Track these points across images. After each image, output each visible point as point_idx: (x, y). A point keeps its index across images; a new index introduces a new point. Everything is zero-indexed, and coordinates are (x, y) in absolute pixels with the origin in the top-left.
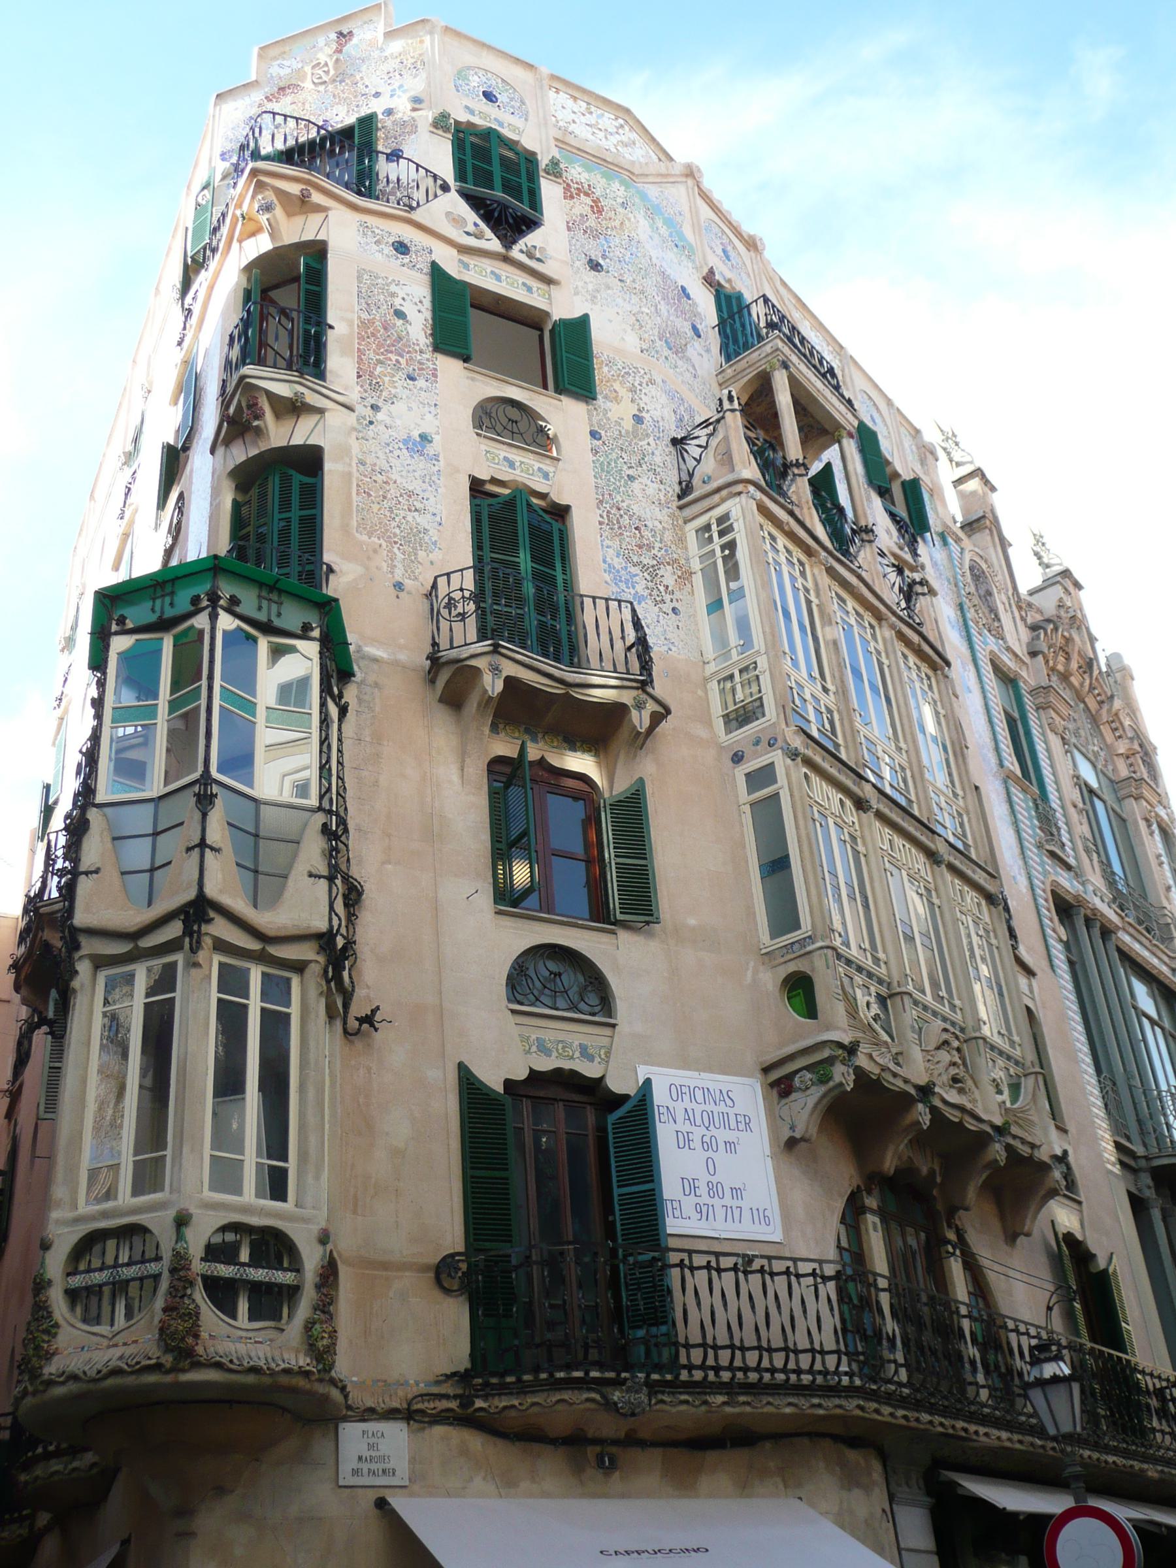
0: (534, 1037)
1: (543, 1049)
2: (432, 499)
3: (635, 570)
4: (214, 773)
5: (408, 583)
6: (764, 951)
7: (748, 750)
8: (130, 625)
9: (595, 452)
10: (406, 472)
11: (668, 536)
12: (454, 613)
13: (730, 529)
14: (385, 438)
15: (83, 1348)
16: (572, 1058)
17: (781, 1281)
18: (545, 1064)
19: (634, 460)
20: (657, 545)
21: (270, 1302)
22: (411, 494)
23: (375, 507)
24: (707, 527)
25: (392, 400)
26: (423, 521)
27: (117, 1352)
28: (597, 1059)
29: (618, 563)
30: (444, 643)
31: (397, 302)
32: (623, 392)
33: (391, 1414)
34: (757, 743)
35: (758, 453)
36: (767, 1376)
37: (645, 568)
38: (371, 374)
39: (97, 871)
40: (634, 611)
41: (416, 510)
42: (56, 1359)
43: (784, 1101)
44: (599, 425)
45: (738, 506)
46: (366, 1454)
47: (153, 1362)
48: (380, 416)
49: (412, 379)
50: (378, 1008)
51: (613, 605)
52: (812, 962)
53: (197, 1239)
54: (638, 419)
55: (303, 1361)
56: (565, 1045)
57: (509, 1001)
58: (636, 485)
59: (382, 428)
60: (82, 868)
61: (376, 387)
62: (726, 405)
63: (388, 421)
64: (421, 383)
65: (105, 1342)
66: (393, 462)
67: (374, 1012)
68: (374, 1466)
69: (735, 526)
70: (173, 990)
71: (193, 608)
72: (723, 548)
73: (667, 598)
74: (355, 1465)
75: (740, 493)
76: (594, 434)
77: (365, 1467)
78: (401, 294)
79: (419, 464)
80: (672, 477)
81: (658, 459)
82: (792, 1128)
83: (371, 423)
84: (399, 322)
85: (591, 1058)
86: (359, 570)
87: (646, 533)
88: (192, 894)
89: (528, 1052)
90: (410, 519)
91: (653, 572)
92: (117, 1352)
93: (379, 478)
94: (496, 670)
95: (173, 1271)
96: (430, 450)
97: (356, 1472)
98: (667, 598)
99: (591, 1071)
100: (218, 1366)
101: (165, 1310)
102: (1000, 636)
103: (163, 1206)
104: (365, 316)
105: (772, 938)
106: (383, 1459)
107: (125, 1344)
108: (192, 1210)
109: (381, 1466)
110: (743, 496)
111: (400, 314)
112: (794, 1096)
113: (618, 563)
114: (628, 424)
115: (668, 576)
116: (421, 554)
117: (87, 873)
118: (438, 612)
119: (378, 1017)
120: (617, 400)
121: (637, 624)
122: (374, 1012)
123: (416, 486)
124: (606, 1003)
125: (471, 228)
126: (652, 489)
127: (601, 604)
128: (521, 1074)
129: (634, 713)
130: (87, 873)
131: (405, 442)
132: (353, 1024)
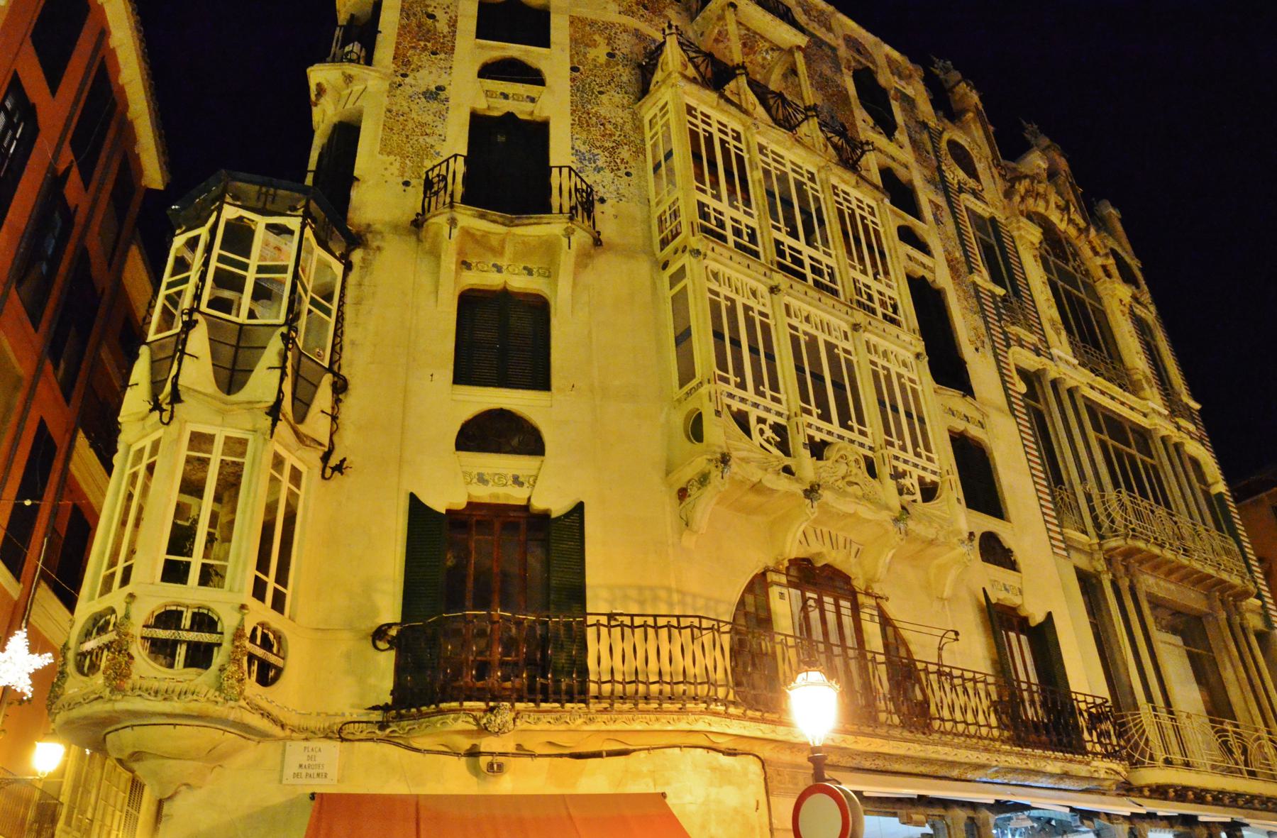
0: (475, 472)
1: (482, 479)
2: (440, 127)
9: (573, 80)
11: (628, 127)
16: (505, 485)
22: (423, 125)
23: (395, 137)
28: (526, 485)
29: (583, 148)
31: (430, 10)
34: (676, 252)
37: (605, 149)
38: (405, 56)
44: (579, 62)
46: (305, 762)
48: (407, 80)
50: (345, 459)
54: (611, 55)
56: (498, 479)
58: (604, 98)
59: (408, 87)
61: (407, 63)
62: (667, 31)
63: (413, 82)
66: (413, 106)
68: (310, 771)
73: (622, 167)
74: (297, 770)
76: (574, 69)
77: (304, 772)
81: (625, 79)
87: (609, 126)
89: (470, 483)
90: (421, 140)
96: (442, 95)
97: (296, 775)
98: (622, 167)
104: (405, 22)
109: (316, 771)
111: (432, 17)
114: (603, 59)
115: (625, 153)
120: (595, 45)
123: (429, 119)
126: (617, 98)
131: (424, 94)
132: (328, 471)
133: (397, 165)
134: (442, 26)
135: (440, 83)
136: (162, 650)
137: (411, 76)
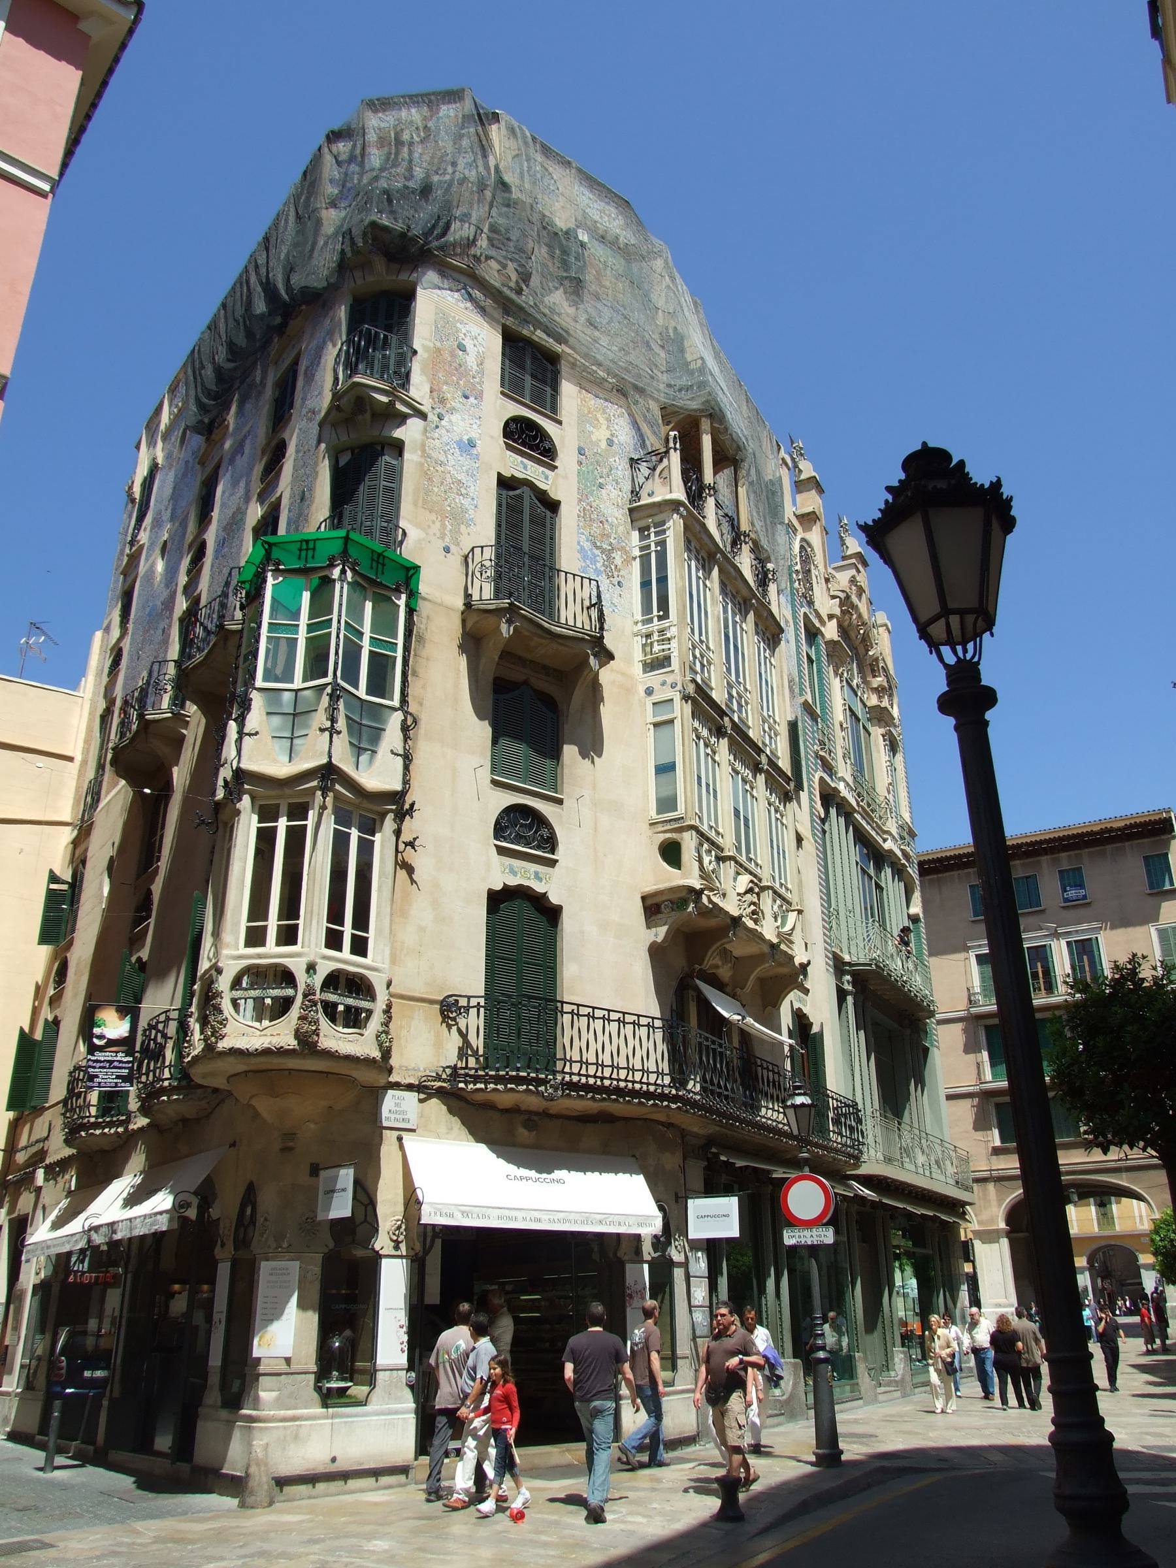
1: (513, 872)
3: (597, 552)
4: (339, 681)
5: (453, 548)
9: (580, 463)
10: (456, 465)
12: (484, 575)
14: (445, 439)
17: (644, 1030)
18: (513, 881)
19: (605, 471)
20: (613, 536)
21: (354, 1019)
23: (436, 489)
25: (452, 410)
26: (466, 502)
27: (262, 1039)
30: (476, 597)
32: (602, 420)
33: (410, 1087)
35: (686, 479)
36: (630, 1085)
38: (440, 390)
39: (257, 733)
40: (598, 587)
46: (394, 1109)
49: (467, 397)
53: (318, 980)
54: (610, 443)
55: (376, 1054)
57: (496, 837)
59: (443, 431)
60: (246, 730)
61: (442, 401)
64: (472, 399)
67: (415, 839)
68: (397, 1116)
70: (306, 819)
72: (657, 544)
76: (581, 452)
77: (393, 1116)
78: (464, 331)
79: (466, 462)
80: (627, 487)
83: (437, 427)
85: (540, 880)
86: (422, 535)
88: (325, 761)
91: (608, 553)
93: (439, 468)
95: (305, 996)
96: (474, 451)
98: (616, 574)
99: (539, 888)
101: (299, 1018)
102: (811, 603)
103: (298, 955)
105: (658, 813)
106: (404, 1112)
108: (319, 961)
109: (401, 1117)
111: (462, 348)
112: (660, 916)
113: (587, 545)
114: (604, 445)
116: (463, 527)
117: (250, 735)
118: (473, 573)
119: (416, 843)
121: (599, 596)
122: (415, 839)
124: (551, 843)
125: (512, 285)
127: (578, 579)
128: (498, 886)
130: (250, 735)
131: (459, 443)
133: (438, 524)
134: (471, 361)
135: (473, 435)
136: (330, 1010)
137: (446, 419)
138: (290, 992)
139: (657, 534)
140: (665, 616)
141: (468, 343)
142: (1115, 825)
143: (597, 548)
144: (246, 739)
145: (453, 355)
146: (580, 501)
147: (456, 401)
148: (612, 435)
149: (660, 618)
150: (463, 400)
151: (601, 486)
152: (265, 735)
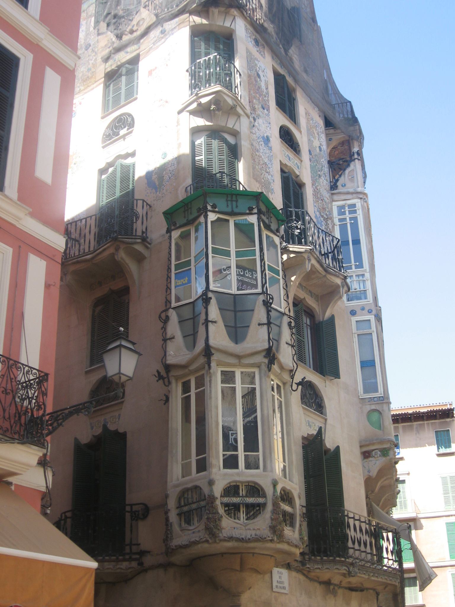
6: (360, 397)
7: (358, 311)
8: (217, 210)
13: (355, 212)
15: (234, 528)
23: (257, 167)
24: (343, 207)
25: (259, 116)
26: (269, 177)
34: (363, 309)
39: (215, 322)
41: (267, 172)
42: (223, 531)
43: (366, 460)
45: (360, 204)
46: (279, 580)
47: (270, 538)
49: (264, 109)
51: (335, 239)
52: (383, 407)
59: (256, 129)
64: (266, 110)
65: (244, 528)
69: (358, 211)
71: (248, 212)
75: (361, 198)
82: (369, 471)
84: (259, 79)
92: (253, 533)
94: (309, 260)
100: (288, 543)
107: (254, 529)
110: (362, 200)
111: (259, 76)
112: (370, 459)
114: (318, 149)
117: (212, 322)
123: (266, 160)
129: (341, 289)
130: (212, 322)
131: (263, 137)
138: (261, 500)
139: (350, 212)
140: (360, 266)
141: (260, 73)
142: (422, 410)
143: (322, 216)
144: (210, 325)
145: (256, 81)
146: (313, 185)
147: (260, 111)
148: (321, 144)
149: (357, 267)
150: (262, 110)
151: (320, 176)
152: (221, 324)
